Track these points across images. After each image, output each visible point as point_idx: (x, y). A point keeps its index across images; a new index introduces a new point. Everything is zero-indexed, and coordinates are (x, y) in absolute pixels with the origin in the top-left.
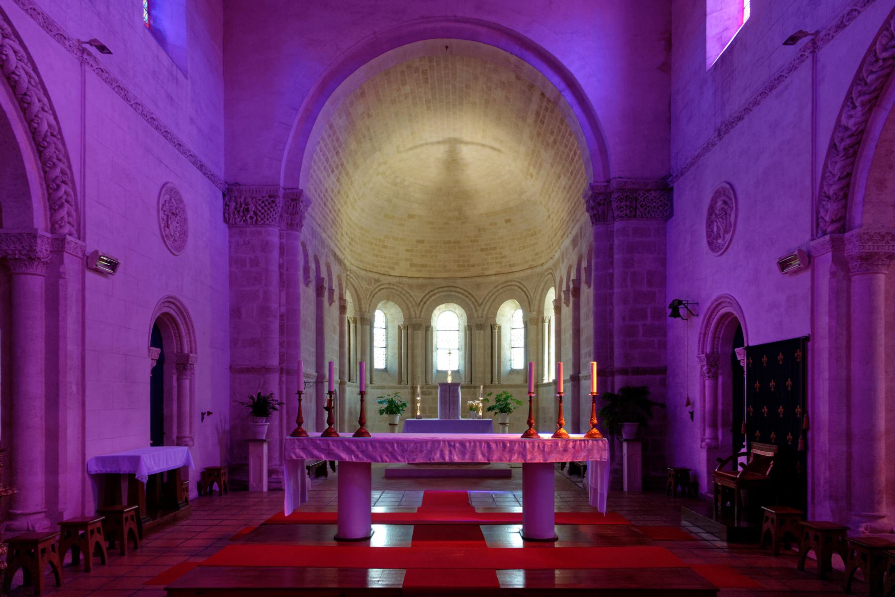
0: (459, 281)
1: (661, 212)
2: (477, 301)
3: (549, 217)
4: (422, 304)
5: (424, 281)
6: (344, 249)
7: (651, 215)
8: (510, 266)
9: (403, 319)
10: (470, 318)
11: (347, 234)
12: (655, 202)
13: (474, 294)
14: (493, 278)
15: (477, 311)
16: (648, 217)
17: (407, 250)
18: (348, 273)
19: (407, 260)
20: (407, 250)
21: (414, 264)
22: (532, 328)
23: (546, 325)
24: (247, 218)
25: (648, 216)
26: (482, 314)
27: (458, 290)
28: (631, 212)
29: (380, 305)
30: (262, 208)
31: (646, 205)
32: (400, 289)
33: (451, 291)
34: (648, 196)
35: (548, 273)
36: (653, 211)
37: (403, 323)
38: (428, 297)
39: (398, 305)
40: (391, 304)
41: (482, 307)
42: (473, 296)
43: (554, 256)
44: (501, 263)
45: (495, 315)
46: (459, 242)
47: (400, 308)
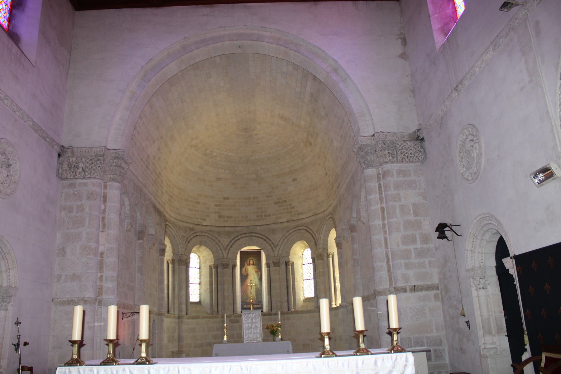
0: (258, 228)
1: (417, 157)
2: (273, 243)
3: (326, 174)
4: (229, 247)
5: (230, 229)
6: (164, 204)
7: (409, 160)
8: (299, 214)
9: (213, 260)
11: (167, 192)
12: (411, 150)
13: (271, 239)
14: (286, 224)
15: (273, 251)
16: (407, 162)
17: (216, 205)
18: (167, 223)
19: (216, 213)
20: (216, 205)
21: (222, 216)
23: (331, 259)
24: (76, 173)
25: (407, 160)
26: (278, 253)
28: (393, 158)
29: (194, 249)
30: (90, 164)
31: (404, 152)
32: (211, 236)
34: (405, 146)
35: (329, 217)
36: (411, 157)
37: (213, 263)
38: (233, 241)
39: (209, 249)
40: (203, 248)
41: (278, 247)
42: (269, 240)
43: (333, 203)
44: (291, 212)
45: (288, 254)
46: (257, 198)
47: (211, 251)
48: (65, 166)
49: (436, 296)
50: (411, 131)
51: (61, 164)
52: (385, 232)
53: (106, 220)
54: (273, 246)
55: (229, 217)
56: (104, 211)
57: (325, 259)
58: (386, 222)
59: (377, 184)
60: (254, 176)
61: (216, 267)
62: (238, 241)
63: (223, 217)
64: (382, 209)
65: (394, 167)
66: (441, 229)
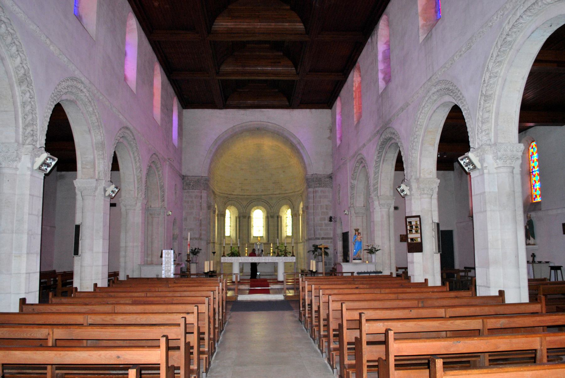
0: (263, 196)
4: (246, 207)
5: (248, 197)
8: (285, 190)
9: (238, 214)
10: (268, 213)
14: (278, 196)
15: (271, 210)
19: (240, 187)
20: (240, 184)
22: (294, 217)
27: (262, 200)
29: (228, 208)
32: (237, 200)
33: (260, 201)
42: (269, 203)
44: (281, 189)
45: (279, 211)
46: (263, 180)
48: (185, 184)
49: (331, 242)
50: (328, 174)
51: (183, 183)
52: (314, 215)
53: (202, 207)
54: (271, 207)
55: (246, 190)
56: (201, 203)
57: (298, 216)
58: (315, 211)
59: (313, 195)
60: (262, 168)
61: (239, 217)
62: (252, 204)
63: (244, 190)
64: (314, 206)
65: (319, 189)
66: (331, 219)
